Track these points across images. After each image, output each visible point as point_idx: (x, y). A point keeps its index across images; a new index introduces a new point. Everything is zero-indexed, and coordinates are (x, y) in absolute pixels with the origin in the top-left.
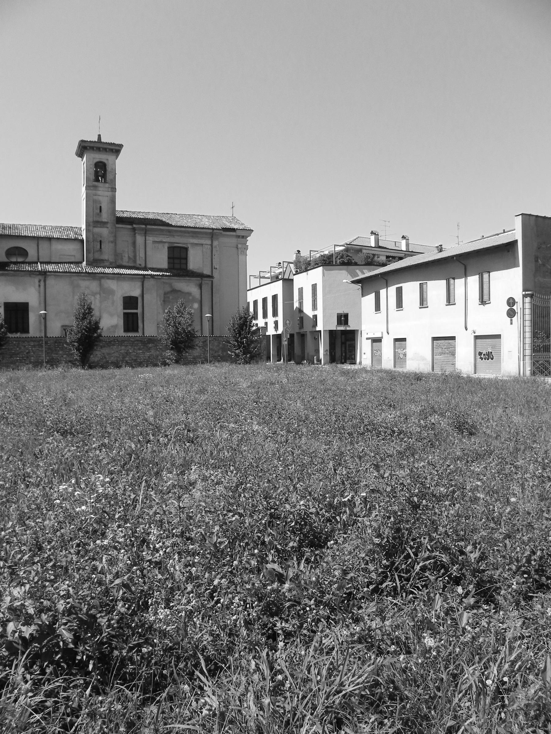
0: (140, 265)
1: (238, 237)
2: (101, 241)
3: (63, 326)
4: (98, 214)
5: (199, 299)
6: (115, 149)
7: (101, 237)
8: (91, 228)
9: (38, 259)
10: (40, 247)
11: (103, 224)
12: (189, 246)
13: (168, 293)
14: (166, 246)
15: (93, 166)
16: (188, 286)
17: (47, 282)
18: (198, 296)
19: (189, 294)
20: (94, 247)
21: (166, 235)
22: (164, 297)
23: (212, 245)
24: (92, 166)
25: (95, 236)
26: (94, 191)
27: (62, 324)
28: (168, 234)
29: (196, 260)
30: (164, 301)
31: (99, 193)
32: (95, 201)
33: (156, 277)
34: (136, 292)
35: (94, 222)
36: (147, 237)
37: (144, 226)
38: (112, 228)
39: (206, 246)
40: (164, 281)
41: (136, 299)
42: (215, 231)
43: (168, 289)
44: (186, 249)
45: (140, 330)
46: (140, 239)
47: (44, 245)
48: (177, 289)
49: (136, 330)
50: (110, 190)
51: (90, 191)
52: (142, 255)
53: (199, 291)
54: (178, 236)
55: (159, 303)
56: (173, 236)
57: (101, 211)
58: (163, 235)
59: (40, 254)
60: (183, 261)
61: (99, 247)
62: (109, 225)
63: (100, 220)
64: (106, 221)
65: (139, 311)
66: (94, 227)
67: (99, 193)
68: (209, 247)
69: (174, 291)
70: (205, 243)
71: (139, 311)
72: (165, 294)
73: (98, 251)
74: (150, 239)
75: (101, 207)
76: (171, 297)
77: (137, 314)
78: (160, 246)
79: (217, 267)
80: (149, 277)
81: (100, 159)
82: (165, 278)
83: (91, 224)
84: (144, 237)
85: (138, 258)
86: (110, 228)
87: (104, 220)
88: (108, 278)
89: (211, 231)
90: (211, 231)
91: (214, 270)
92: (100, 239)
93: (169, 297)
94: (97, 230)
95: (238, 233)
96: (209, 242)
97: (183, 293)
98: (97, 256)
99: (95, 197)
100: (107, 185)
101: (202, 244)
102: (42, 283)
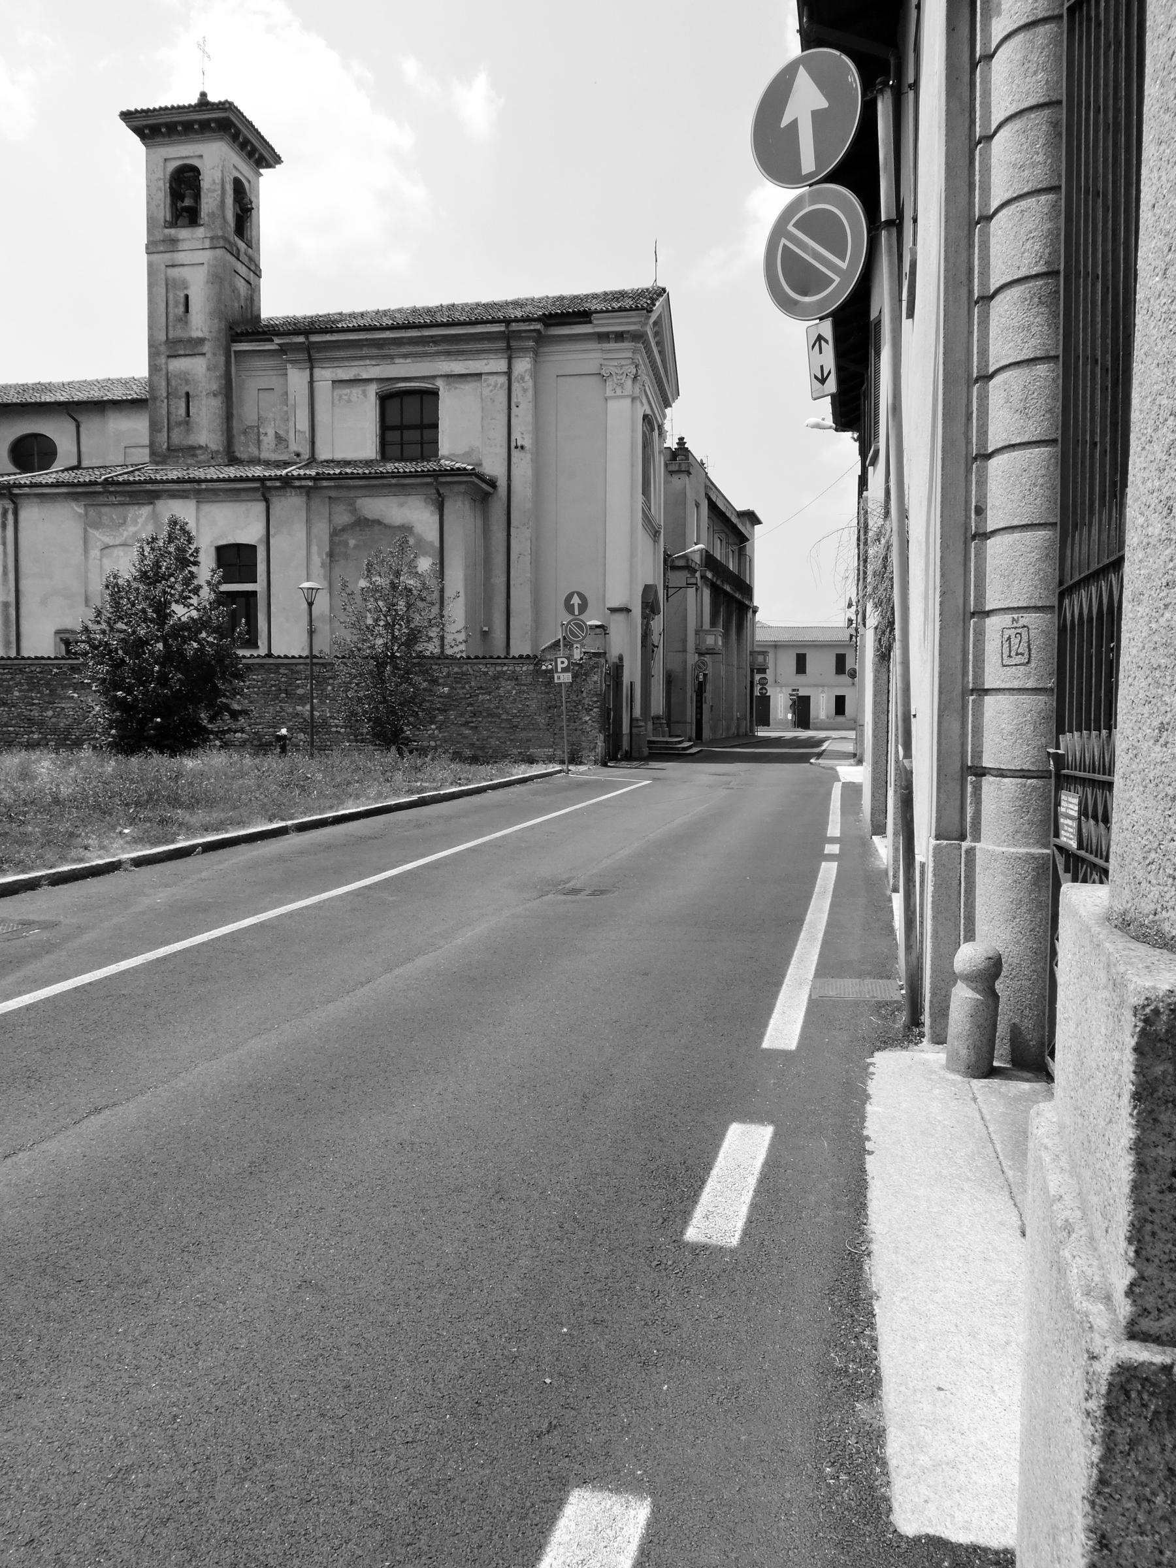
0: (298, 455)
1: (603, 337)
2: (188, 394)
3: (57, 632)
4: (180, 320)
5: (437, 544)
6: (219, 121)
7: (187, 382)
8: (162, 360)
9: (79, 461)
10: (81, 429)
11: (192, 347)
12: (440, 383)
13: (344, 529)
14: (372, 389)
15: (163, 186)
16: (401, 505)
17: (24, 514)
18: (432, 536)
19: (407, 529)
20: (168, 413)
21: (371, 358)
22: (332, 543)
23: (509, 374)
24: (161, 183)
25: (173, 383)
26: (167, 256)
27: (59, 627)
28: (374, 352)
29: (464, 429)
30: (331, 555)
31: (181, 257)
32: (170, 284)
33: (297, 483)
34: (249, 532)
35: (168, 344)
36: (317, 372)
37: (301, 339)
38: (214, 354)
39: (492, 380)
40: (333, 494)
41: (253, 548)
42: (514, 327)
43: (343, 517)
44: (434, 394)
45: (262, 642)
46: (297, 378)
47: (91, 426)
48: (369, 516)
49: (255, 646)
50: (207, 244)
51: (155, 257)
52: (303, 424)
53: (437, 517)
54: (405, 356)
55: (316, 560)
56: (391, 357)
57: (187, 310)
58: (362, 358)
59: (83, 449)
60: (427, 433)
61: (182, 411)
62: (206, 348)
63: (185, 335)
64: (200, 335)
65: (259, 587)
66: (169, 357)
67: (181, 257)
68: (503, 380)
69: (363, 523)
70: (486, 369)
71: (259, 587)
72: (334, 533)
73: (179, 424)
74: (325, 375)
75: (187, 297)
76: (352, 543)
77: (254, 594)
78: (356, 392)
79: (527, 442)
80: (278, 484)
81: (203, 162)
82: (325, 483)
83: (163, 348)
84: (308, 372)
85: (292, 434)
86: (209, 355)
87: (196, 334)
88: (173, 495)
89: (500, 328)
90: (500, 328)
91: (515, 454)
92: (187, 389)
93: (346, 544)
94: (177, 365)
95: (601, 325)
96: (501, 365)
97: (387, 527)
98: (177, 437)
99: (173, 272)
100: (200, 232)
101: (480, 375)
102: (10, 517)
